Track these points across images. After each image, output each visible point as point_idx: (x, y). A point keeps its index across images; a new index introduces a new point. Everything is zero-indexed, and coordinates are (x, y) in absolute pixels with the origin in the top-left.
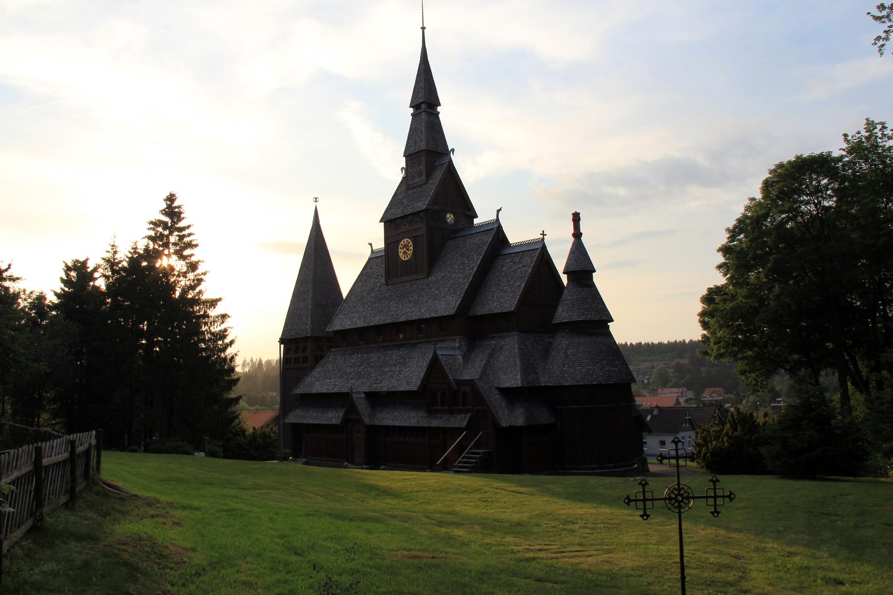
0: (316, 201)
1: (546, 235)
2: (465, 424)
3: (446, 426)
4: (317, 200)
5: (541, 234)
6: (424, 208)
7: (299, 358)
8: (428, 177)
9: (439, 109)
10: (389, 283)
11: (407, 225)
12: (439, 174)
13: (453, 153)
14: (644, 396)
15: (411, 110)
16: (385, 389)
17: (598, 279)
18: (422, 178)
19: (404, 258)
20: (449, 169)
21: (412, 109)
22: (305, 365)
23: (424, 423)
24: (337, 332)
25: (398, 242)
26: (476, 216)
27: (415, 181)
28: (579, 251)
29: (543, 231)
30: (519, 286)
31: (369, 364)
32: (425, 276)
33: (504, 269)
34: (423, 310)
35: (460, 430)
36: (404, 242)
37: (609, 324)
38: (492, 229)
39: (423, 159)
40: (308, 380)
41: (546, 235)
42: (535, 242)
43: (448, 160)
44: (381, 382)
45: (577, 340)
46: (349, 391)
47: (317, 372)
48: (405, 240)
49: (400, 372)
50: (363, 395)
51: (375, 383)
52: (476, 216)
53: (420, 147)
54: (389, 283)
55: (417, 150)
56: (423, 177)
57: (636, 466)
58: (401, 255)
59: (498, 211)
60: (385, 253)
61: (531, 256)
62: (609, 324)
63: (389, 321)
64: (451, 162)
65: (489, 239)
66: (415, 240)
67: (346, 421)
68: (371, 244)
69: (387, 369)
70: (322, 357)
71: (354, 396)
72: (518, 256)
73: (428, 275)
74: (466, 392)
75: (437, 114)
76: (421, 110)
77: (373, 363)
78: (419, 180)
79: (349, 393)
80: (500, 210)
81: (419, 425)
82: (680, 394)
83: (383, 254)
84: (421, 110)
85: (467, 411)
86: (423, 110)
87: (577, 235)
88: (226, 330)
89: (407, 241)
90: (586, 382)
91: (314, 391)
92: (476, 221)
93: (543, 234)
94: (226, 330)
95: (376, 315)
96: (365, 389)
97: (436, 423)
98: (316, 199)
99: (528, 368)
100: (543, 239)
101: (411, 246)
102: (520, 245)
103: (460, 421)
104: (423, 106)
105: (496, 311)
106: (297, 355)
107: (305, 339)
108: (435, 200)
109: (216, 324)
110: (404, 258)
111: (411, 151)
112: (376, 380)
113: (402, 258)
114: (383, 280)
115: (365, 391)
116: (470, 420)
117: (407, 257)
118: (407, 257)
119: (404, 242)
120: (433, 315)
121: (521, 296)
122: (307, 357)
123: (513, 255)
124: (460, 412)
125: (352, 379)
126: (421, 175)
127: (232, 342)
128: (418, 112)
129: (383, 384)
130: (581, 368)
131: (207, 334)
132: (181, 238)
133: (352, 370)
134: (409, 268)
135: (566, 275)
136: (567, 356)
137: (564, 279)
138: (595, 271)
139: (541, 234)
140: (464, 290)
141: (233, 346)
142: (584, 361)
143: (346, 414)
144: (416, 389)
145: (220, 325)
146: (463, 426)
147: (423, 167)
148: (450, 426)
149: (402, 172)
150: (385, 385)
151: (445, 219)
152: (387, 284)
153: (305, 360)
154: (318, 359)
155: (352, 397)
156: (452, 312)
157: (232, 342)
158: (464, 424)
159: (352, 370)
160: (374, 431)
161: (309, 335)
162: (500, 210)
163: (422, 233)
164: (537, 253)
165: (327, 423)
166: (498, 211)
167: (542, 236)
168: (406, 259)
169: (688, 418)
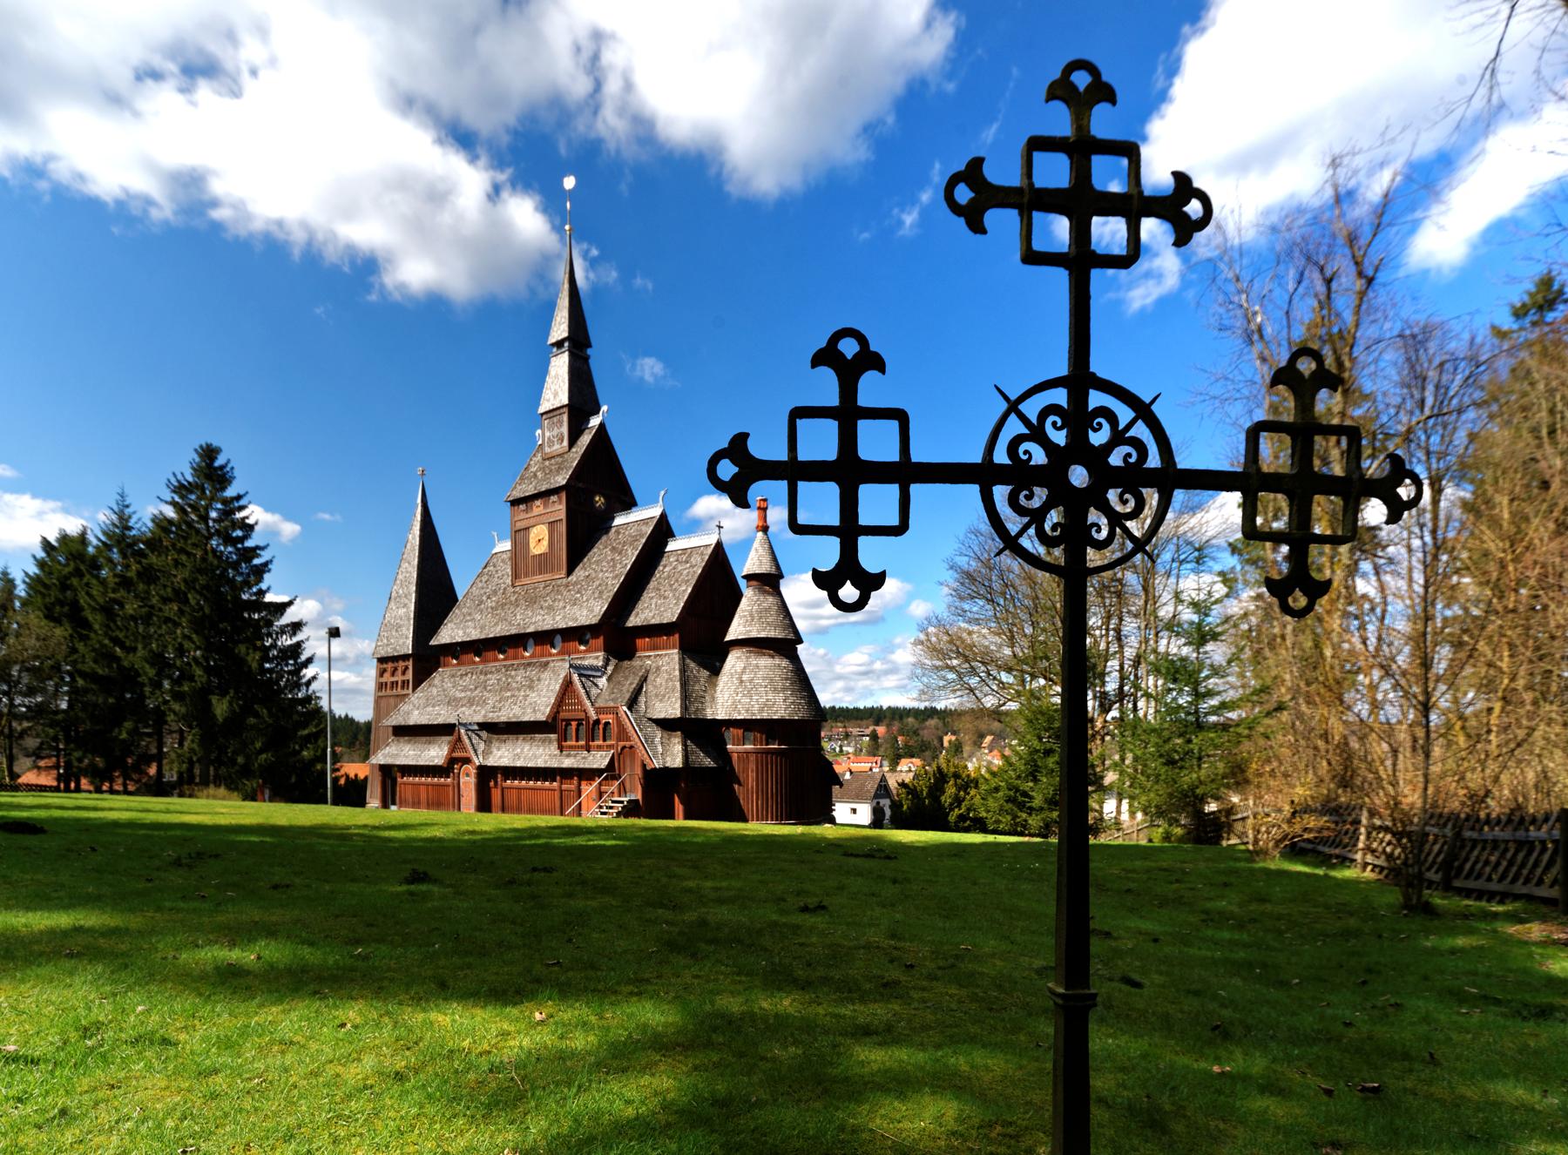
3: (581, 766)
8: (572, 443)
9: (589, 351)
12: (585, 439)
16: (504, 719)
22: (405, 692)
30: (685, 591)
31: (485, 688)
33: (667, 569)
34: (558, 618)
35: (598, 772)
39: (565, 418)
40: (405, 708)
47: (418, 697)
49: (526, 696)
56: (566, 443)
58: (532, 545)
61: (702, 554)
69: (509, 694)
73: (570, 572)
75: (586, 359)
81: (547, 765)
85: (610, 747)
90: (765, 716)
91: (411, 722)
95: (497, 624)
96: (479, 718)
97: (567, 763)
103: (599, 760)
104: (566, 344)
105: (653, 622)
114: (509, 581)
116: (612, 759)
120: (571, 624)
121: (686, 603)
124: (599, 748)
129: (503, 712)
133: (463, 695)
134: (544, 563)
136: (742, 682)
137: (742, 583)
140: (612, 594)
143: (452, 750)
147: (565, 429)
148: (587, 766)
150: (506, 714)
151: (593, 502)
156: (595, 621)
158: (604, 763)
159: (463, 695)
160: (486, 775)
164: (710, 551)
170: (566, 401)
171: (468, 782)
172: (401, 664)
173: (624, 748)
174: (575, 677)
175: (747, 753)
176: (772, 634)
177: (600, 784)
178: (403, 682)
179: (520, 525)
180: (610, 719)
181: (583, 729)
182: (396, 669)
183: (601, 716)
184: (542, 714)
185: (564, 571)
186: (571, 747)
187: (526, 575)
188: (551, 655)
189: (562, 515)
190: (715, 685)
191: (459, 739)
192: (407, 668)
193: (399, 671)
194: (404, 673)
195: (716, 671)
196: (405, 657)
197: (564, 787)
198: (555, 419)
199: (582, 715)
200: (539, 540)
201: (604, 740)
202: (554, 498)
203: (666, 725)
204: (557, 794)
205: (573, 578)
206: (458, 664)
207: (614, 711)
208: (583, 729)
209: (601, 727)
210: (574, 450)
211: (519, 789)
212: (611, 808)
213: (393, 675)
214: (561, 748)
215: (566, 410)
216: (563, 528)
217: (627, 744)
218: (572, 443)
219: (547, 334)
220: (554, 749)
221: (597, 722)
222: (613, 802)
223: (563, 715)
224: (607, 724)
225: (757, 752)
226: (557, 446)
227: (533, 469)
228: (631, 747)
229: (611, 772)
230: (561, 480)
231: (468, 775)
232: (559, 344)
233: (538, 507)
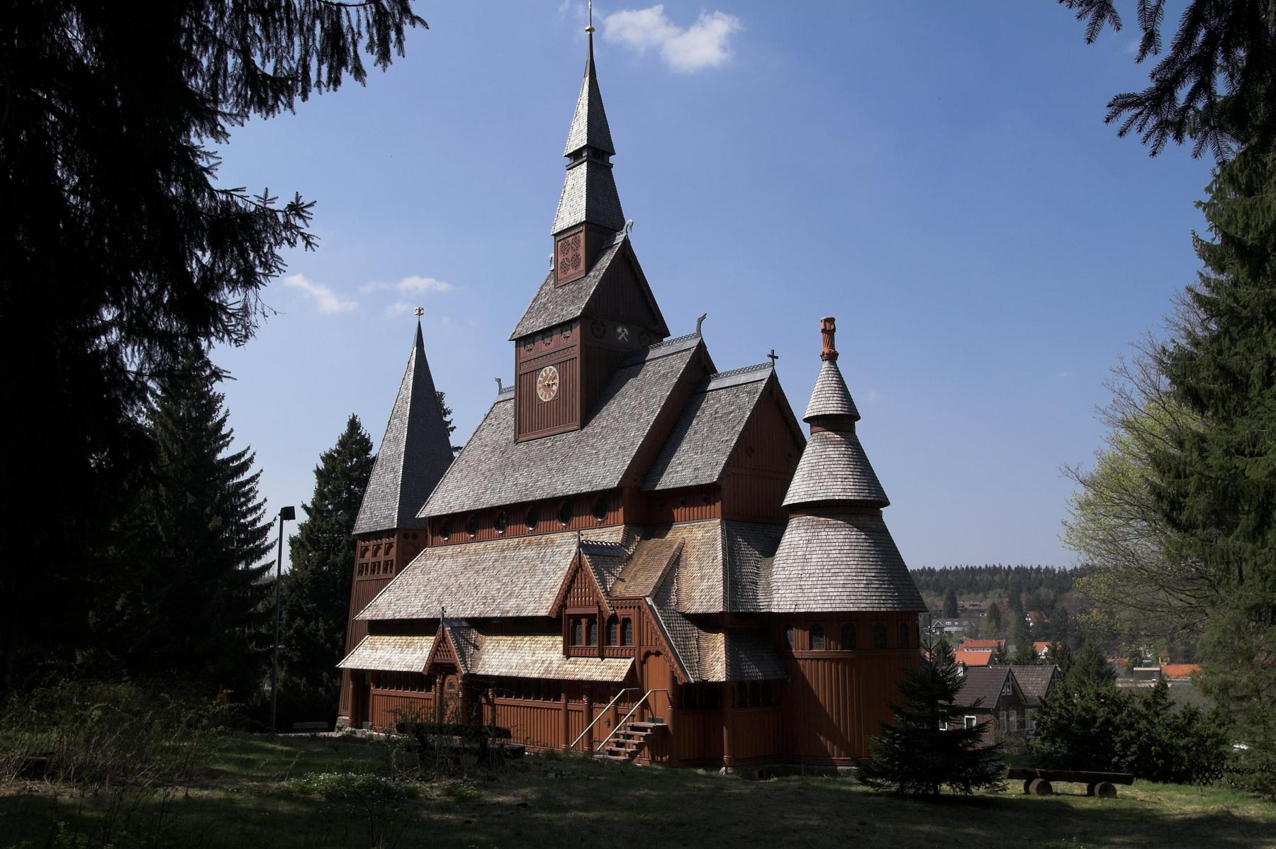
1: (777, 358)
4: (422, 312)
5: (770, 356)
9: (612, 159)
10: (521, 439)
12: (606, 261)
20: (623, 255)
32: (576, 427)
36: (545, 371)
39: (582, 235)
41: (777, 358)
45: (823, 533)
48: (547, 368)
54: (521, 439)
56: (582, 266)
58: (539, 392)
68: (499, 381)
73: (582, 427)
80: (704, 317)
89: (550, 369)
93: (773, 357)
98: (420, 310)
99: (734, 582)
103: (614, 669)
114: (511, 436)
118: (549, 397)
119: (545, 371)
128: (576, 163)
138: (858, 418)
139: (770, 356)
144: (547, 614)
152: (517, 442)
162: (704, 317)
168: (548, 400)
170: (581, 217)
172: (385, 541)
174: (586, 559)
176: (849, 495)
177: (617, 703)
179: (525, 369)
180: (632, 614)
181: (596, 629)
182: (379, 547)
183: (619, 612)
184: (542, 606)
189: (576, 352)
190: (771, 566)
191: (443, 640)
192: (391, 546)
193: (381, 552)
194: (387, 553)
195: (770, 548)
196: (388, 533)
199: (595, 610)
200: (548, 383)
201: (623, 643)
203: (706, 622)
204: (562, 713)
205: (584, 431)
208: (596, 629)
210: (592, 274)
212: (630, 737)
213: (375, 554)
219: (564, 144)
220: (557, 655)
221: (614, 619)
222: (633, 728)
224: (627, 621)
226: (571, 271)
227: (544, 300)
229: (634, 683)
230: (576, 311)
232: (576, 155)
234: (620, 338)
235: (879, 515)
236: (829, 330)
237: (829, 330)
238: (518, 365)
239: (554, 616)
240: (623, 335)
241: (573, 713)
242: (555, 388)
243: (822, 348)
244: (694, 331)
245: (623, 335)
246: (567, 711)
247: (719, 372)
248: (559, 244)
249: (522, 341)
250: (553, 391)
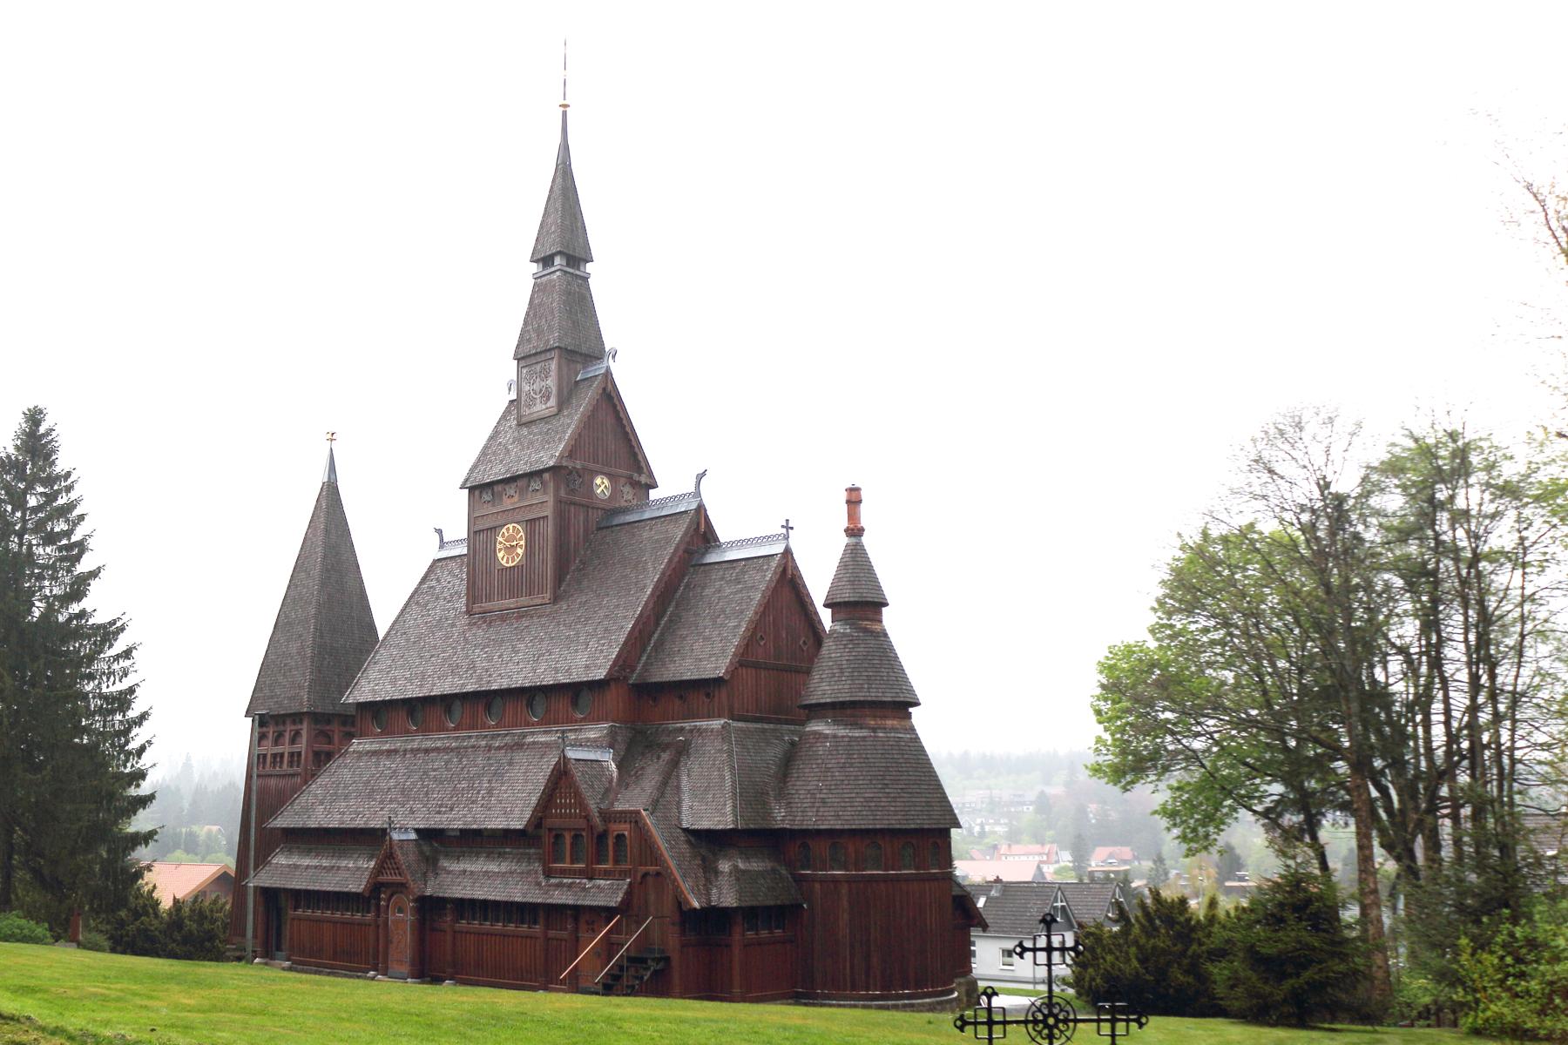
0: (332, 440)
1: (792, 528)
2: (619, 899)
5: (783, 526)
6: (551, 463)
7: (282, 755)
9: (589, 267)
11: (516, 498)
13: (614, 357)
14: (972, 859)
15: (534, 268)
17: (892, 620)
18: (548, 405)
19: (507, 562)
21: (535, 264)
23: (536, 897)
24: (362, 706)
25: (494, 530)
26: (654, 486)
27: (535, 409)
28: (856, 563)
29: (787, 520)
35: (609, 912)
36: (508, 529)
37: (911, 710)
38: (686, 512)
39: (554, 365)
40: (304, 800)
41: (792, 528)
42: (768, 539)
43: (603, 371)
44: (452, 809)
46: (385, 826)
47: (317, 788)
48: (511, 526)
50: (413, 836)
51: (439, 812)
52: (654, 486)
53: (548, 340)
55: (542, 347)
56: (553, 402)
57: (956, 994)
58: (500, 555)
59: (700, 477)
60: (468, 550)
62: (911, 710)
63: (470, 688)
64: (608, 374)
65: (678, 532)
66: (531, 524)
67: (376, 888)
68: (439, 532)
70: (329, 756)
71: (396, 836)
72: (734, 568)
74: (624, 835)
76: (553, 269)
77: (435, 770)
78: (544, 407)
79: (384, 831)
80: (704, 474)
82: (1045, 858)
83: (465, 551)
84: (553, 269)
85: (623, 875)
86: (558, 267)
87: (855, 531)
88: (131, 690)
91: (312, 824)
92: (654, 494)
93: (788, 527)
94: (131, 690)
100: (787, 537)
101: (521, 539)
102: (741, 543)
103: (606, 892)
104: (558, 260)
106: (279, 749)
107: (297, 717)
108: (572, 452)
109: (112, 679)
110: (507, 562)
111: (528, 349)
112: (441, 806)
113: (504, 562)
114: (461, 604)
115: (416, 826)
117: (513, 561)
118: (513, 561)
119: (508, 529)
122: (299, 754)
123: (725, 566)
124: (606, 875)
125: (391, 801)
126: (548, 399)
127: (143, 717)
130: (854, 795)
131: (94, 698)
132: (51, 497)
133: (392, 783)
134: (516, 581)
135: (830, 610)
137: (826, 616)
138: (886, 605)
139: (783, 526)
141: (145, 723)
142: (861, 782)
145: (120, 681)
146: (613, 904)
149: (510, 389)
152: (469, 612)
153: (295, 757)
154: (322, 759)
155: (391, 838)
156: (600, 674)
157: (143, 717)
160: (430, 907)
161: (305, 710)
162: (704, 474)
163: (545, 514)
165: (337, 889)
166: (700, 477)
167: (784, 531)
168: (511, 564)
169: (1059, 904)
171: (401, 920)
172: (289, 728)
173: (645, 875)
175: (835, 880)
178: (292, 755)
185: (548, 596)
186: (564, 873)
187: (489, 599)
188: (528, 724)
189: (548, 511)
197: (552, 933)
198: (538, 367)
199: (582, 823)
200: (510, 548)
201: (616, 862)
202: (536, 485)
206: (382, 734)
207: (633, 818)
209: (611, 842)
211: (479, 934)
214: (548, 874)
215: (555, 354)
216: (549, 529)
217: (652, 869)
218: (563, 403)
223: (549, 822)
224: (620, 837)
225: (850, 880)
228: (658, 874)
231: (400, 911)
233: (511, 499)
234: (599, 491)
235: (909, 716)
236: (854, 499)
237: (854, 499)
238: (472, 520)
239: (530, 829)
240: (603, 486)
241: (485, 937)
242: (520, 551)
243: (844, 523)
244: (692, 489)
245: (603, 486)
246: (548, 939)
247: (722, 540)
248: (525, 371)
249: (478, 490)
250: (518, 555)
